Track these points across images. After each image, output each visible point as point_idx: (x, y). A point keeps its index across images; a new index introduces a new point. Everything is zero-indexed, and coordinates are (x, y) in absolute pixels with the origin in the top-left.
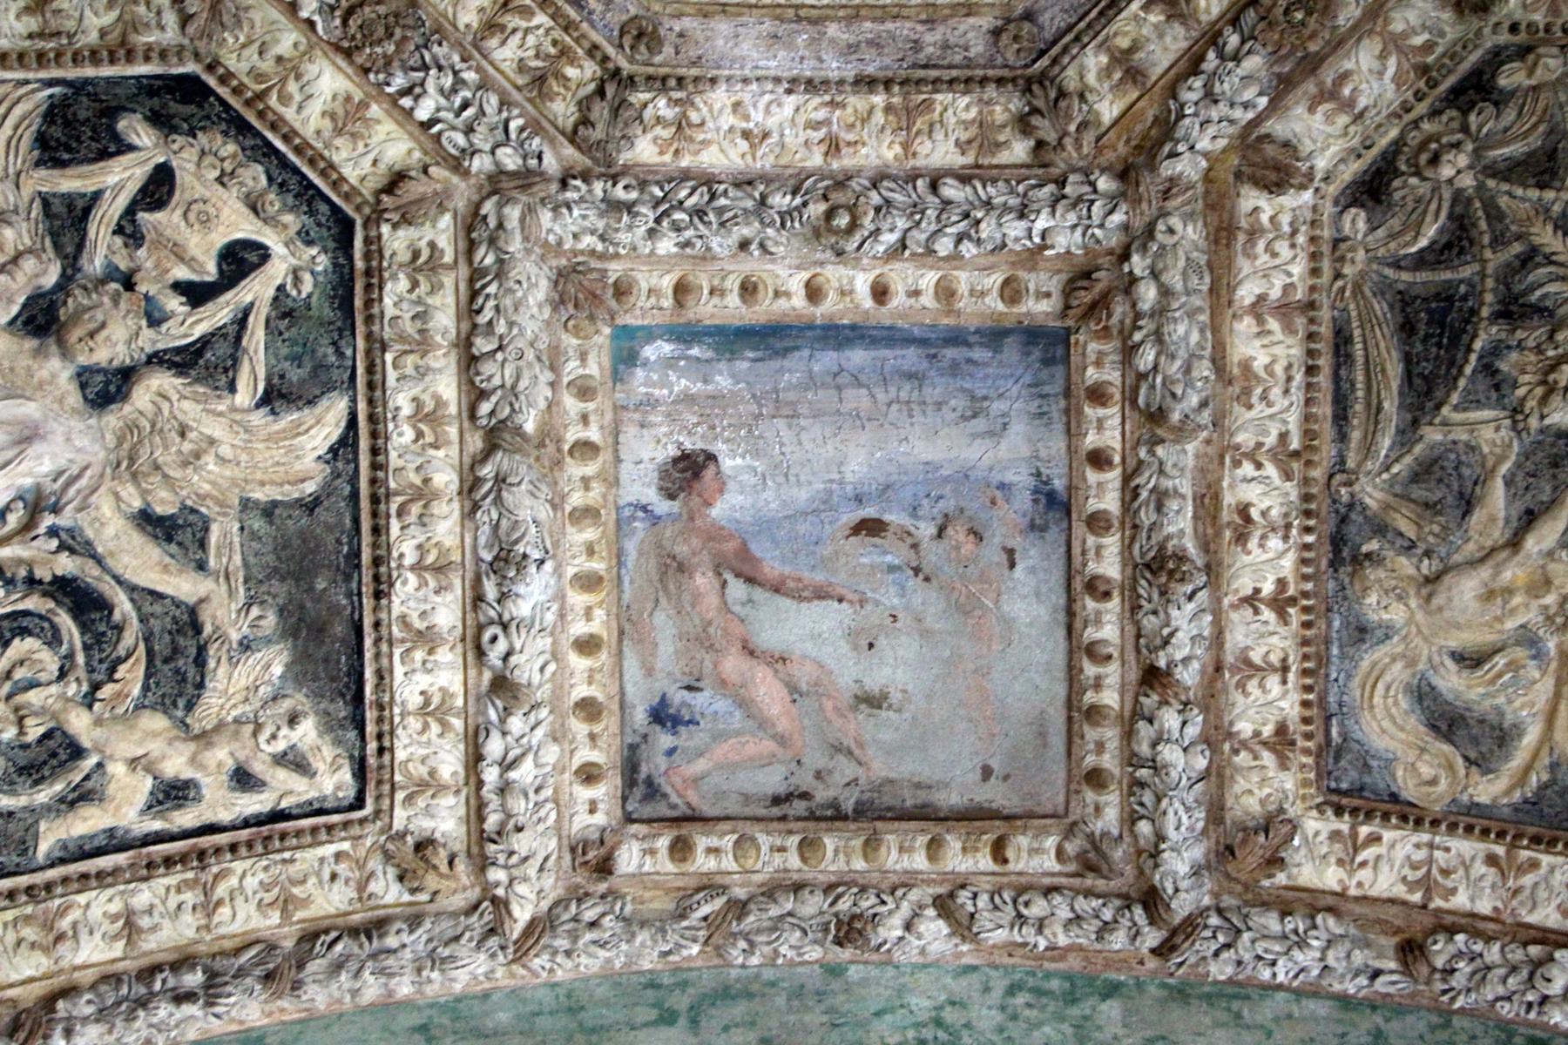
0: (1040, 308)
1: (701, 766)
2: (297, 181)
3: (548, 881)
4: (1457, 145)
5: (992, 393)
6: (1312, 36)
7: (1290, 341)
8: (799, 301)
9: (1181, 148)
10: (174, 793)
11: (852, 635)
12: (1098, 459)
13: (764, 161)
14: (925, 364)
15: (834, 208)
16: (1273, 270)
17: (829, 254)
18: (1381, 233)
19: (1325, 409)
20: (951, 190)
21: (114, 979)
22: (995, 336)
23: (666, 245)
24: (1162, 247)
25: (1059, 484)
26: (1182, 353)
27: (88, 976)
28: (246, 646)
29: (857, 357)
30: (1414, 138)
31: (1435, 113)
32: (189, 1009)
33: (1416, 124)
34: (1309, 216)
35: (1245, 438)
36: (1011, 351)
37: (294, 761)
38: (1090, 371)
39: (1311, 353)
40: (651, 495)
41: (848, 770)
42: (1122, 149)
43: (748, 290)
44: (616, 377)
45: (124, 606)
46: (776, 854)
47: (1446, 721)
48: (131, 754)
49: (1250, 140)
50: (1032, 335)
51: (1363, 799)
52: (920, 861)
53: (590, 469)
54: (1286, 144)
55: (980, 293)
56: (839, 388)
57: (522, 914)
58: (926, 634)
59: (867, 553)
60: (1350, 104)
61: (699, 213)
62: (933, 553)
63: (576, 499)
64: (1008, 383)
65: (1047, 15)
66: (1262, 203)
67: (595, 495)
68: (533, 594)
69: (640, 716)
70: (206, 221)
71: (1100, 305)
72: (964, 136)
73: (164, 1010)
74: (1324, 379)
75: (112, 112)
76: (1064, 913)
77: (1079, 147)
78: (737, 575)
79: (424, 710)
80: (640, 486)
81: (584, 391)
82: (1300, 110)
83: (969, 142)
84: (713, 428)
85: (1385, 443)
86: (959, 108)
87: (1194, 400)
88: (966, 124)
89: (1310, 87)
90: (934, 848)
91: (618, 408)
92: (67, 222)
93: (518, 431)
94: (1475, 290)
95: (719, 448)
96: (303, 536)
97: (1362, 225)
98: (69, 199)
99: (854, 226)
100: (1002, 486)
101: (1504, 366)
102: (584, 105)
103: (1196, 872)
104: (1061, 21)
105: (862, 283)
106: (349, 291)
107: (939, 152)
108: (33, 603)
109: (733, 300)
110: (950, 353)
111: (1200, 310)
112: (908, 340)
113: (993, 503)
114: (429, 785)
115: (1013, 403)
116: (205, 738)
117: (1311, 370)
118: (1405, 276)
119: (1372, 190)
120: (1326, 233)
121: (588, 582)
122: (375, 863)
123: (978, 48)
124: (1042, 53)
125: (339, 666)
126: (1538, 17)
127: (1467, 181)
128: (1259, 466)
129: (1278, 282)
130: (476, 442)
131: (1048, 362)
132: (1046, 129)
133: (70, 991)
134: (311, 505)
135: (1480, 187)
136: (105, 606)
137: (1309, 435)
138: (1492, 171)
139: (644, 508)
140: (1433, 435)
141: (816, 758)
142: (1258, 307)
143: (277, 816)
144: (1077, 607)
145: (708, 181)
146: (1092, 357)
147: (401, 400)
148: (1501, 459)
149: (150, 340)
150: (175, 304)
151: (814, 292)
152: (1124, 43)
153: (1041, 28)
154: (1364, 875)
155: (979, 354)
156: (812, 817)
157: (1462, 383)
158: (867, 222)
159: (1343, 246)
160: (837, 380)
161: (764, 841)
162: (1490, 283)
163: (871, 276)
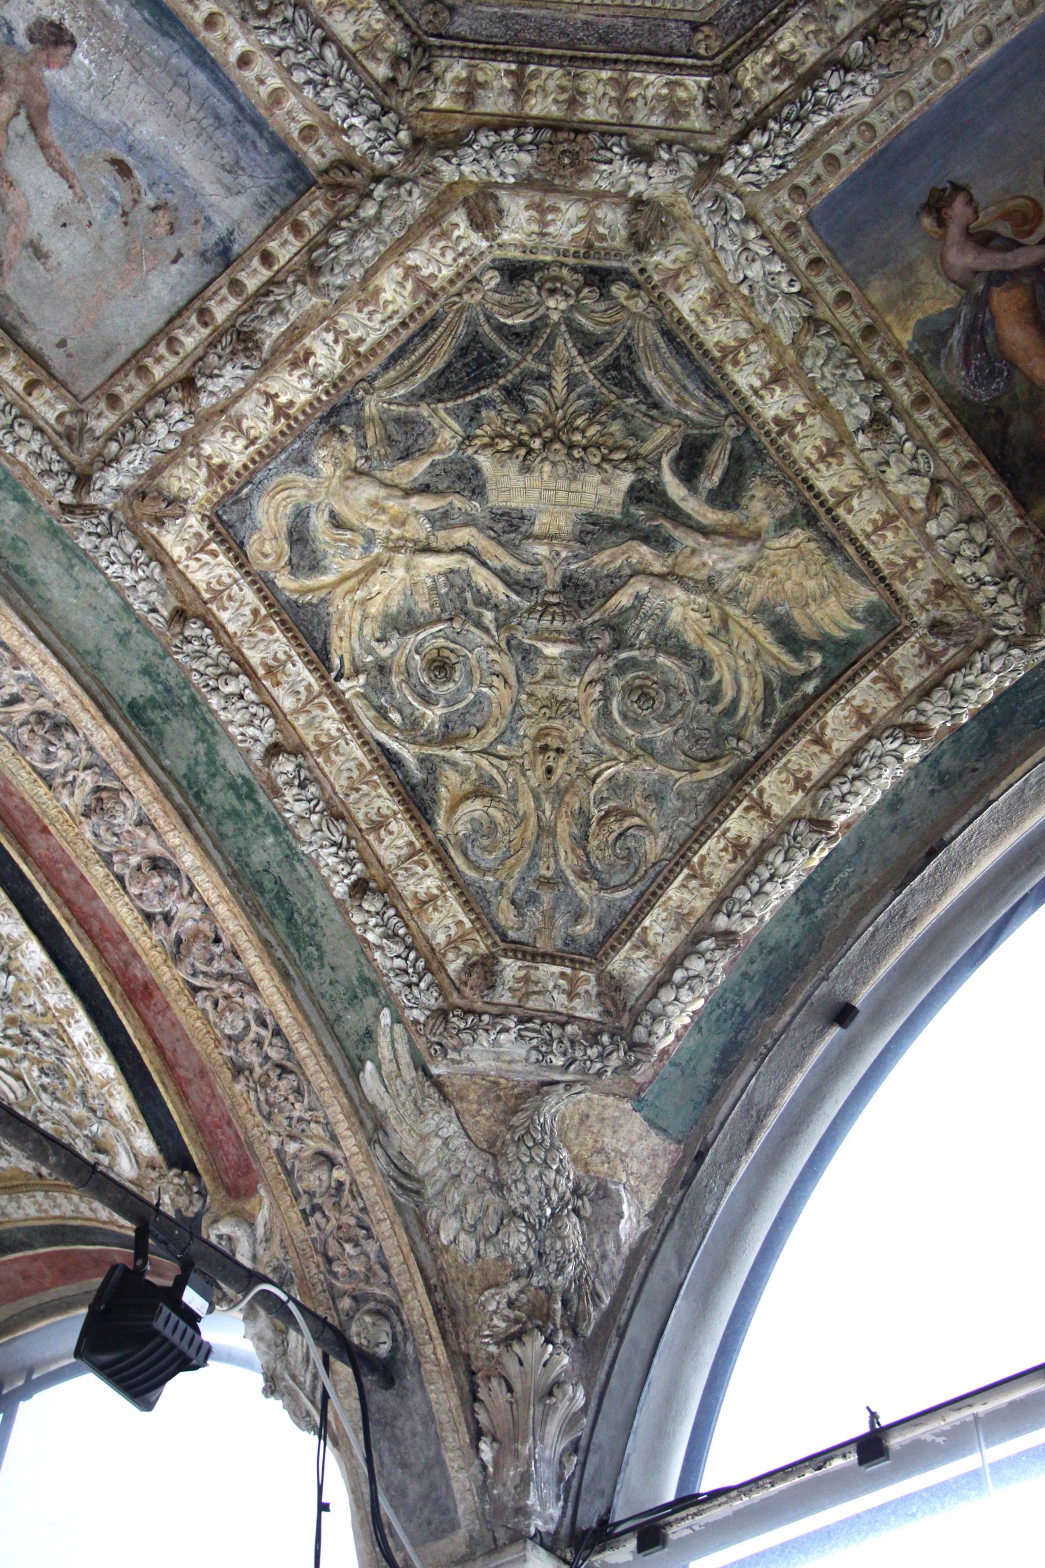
0: (314, 157)
4: (567, 295)
5: (249, 171)
6: (562, 177)
7: (408, 300)
8: (199, 17)
9: (454, 161)
11: (60, 210)
12: (267, 258)
14: (230, 120)
16: (434, 262)
17: (237, 12)
18: (497, 296)
19: (391, 348)
20: (330, 53)
22: (279, 145)
24: (399, 196)
25: (236, 248)
26: (356, 254)
29: (200, 78)
30: (554, 271)
31: (573, 269)
33: (562, 265)
34: (476, 254)
35: (343, 322)
36: (278, 161)
38: (306, 213)
39: (412, 316)
40: (21, 27)
42: (428, 127)
47: (298, 535)
49: (487, 191)
50: (296, 164)
51: (227, 531)
54: (500, 211)
55: (293, 116)
56: (175, 83)
58: (98, 248)
59: (107, 179)
60: (546, 224)
62: (141, 214)
64: (260, 177)
65: (460, 20)
66: (462, 225)
71: (339, 189)
72: (363, 33)
74: (405, 334)
76: (35, 446)
77: (410, 104)
78: (28, 117)
82: (522, 202)
83: (363, 39)
84: (89, 29)
87: (339, 281)
88: (370, 28)
89: (537, 197)
94: (507, 367)
95: (83, 44)
97: (493, 284)
99: (264, 15)
100: (208, 219)
101: (484, 413)
103: (118, 490)
104: (464, 31)
105: (240, 45)
110: (249, 129)
111: (385, 243)
112: (234, 99)
113: (196, 222)
115: (254, 186)
117: (404, 324)
118: (487, 328)
119: (515, 273)
120: (474, 270)
124: (439, 36)
126: (656, 278)
127: (555, 316)
128: (336, 341)
129: (432, 269)
132: (404, 77)
135: (557, 325)
137: (372, 351)
138: (569, 322)
139: (10, 30)
140: (424, 410)
142: (411, 270)
144: (186, 314)
146: (313, 208)
148: (440, 451)
151: (211, 22)
152: (481, 77)
153: (452, 23)
154: (194, 565)
155: (262, 144)
157: (460, 401)
158: (273, 22)
159: (476, 285)
160: (178, 77)
162: (517, 371)
163: (248, 48)
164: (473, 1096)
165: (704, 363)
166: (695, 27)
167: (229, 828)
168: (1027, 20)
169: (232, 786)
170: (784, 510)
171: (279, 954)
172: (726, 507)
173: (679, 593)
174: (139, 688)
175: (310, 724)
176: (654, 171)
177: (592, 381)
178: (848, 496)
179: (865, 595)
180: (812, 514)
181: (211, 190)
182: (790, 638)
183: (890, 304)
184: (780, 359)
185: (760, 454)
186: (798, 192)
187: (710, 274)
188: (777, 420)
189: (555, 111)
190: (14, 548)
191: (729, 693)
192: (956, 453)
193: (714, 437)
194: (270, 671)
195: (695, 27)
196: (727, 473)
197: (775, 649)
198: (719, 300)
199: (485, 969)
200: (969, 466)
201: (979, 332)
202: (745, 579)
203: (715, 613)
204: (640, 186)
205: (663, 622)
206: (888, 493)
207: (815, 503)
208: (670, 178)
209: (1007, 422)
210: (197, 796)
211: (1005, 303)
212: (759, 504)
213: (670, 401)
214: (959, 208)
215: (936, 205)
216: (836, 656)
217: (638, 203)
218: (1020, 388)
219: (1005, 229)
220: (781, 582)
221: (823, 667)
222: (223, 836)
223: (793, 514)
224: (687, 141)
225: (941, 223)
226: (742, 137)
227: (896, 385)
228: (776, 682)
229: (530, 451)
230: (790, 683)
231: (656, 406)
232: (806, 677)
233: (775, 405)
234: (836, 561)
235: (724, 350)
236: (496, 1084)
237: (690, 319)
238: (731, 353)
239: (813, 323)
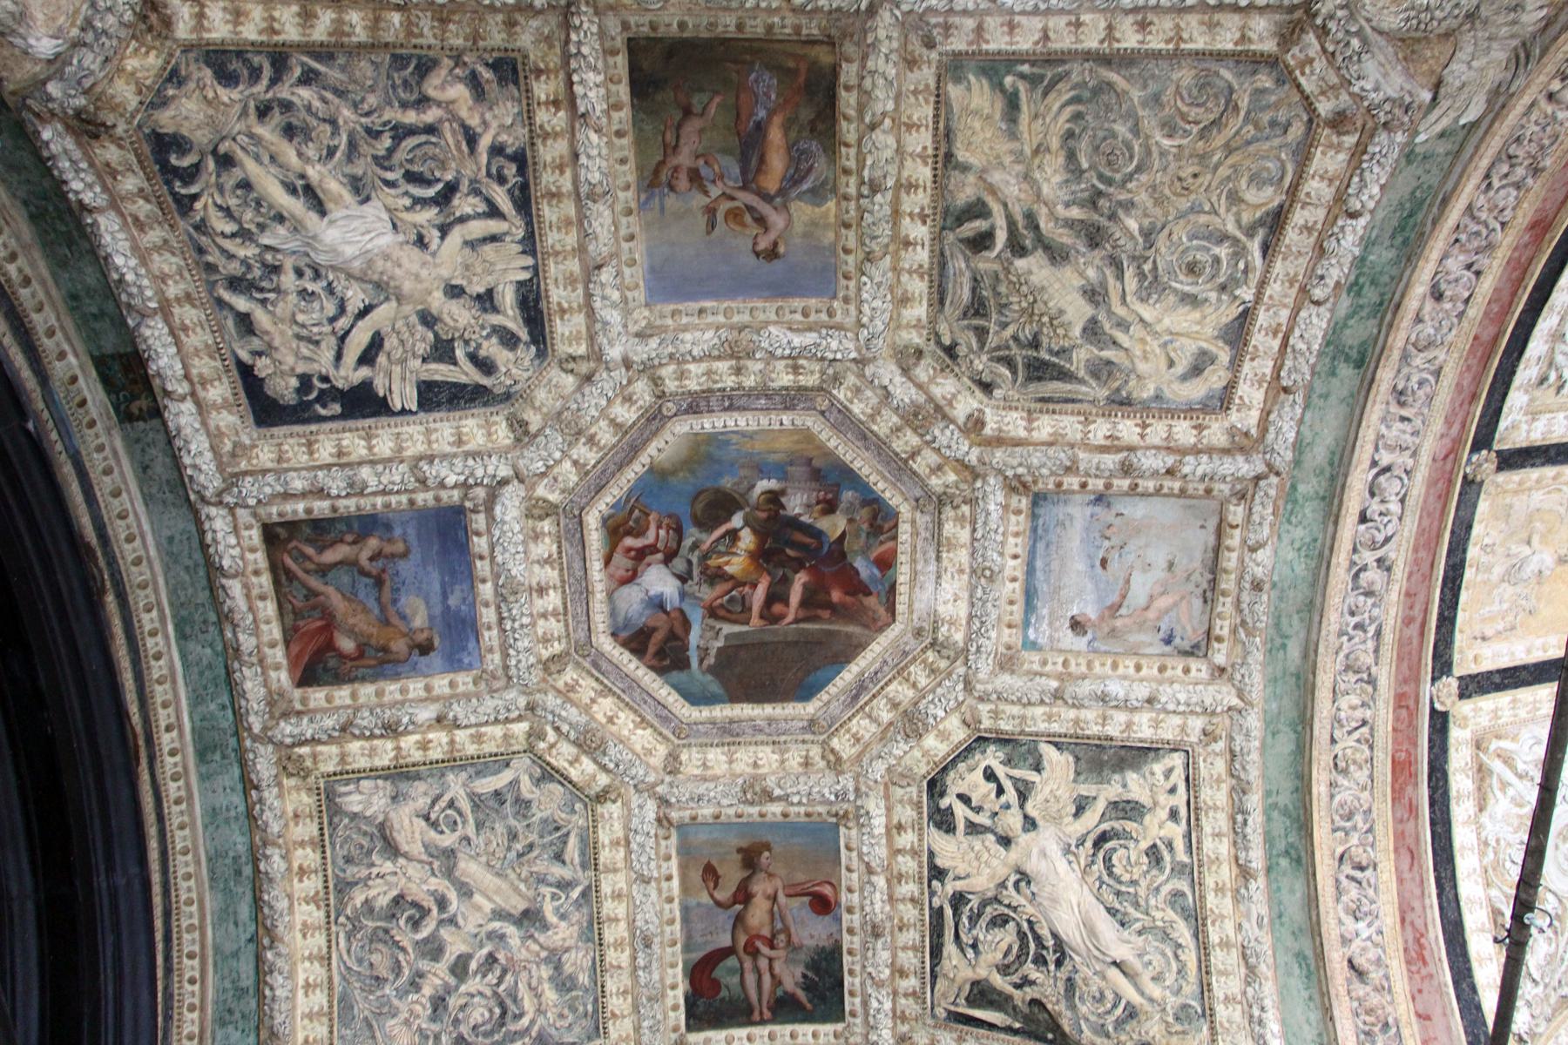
0: (1024, 503)
1: (1189, 628)
2: (965, 753)
3: (1224, 689)
8: (1017, 585)
10: (1174, 815)
11: (1144, 571)
12: (1084, 485)
13: (966, 595)
15: (981, 574)
19: (1070, 406)
20: (979, 535)
21: (1235, 843)
22: (1034, 516)
23: (993, 634)
27: (1233, 851)
28: (1125, 786)
29: (1039, 564)
32: (1250, 822)
35: (1079, 436)
36: (1041, 511)
37: (1168, 773)
40: (1085, 640)
41: (1196, 577)
43: (1011, 603)
44: (1040, 649)
45: (1105, 826)
46: (1225, 606)
47: (1196, 370)
48: (1157, 828)
50: (1035, 504)
51: (1224, 400)
52: (1234, 555)
53: (1073, 662)
55: (1019, 522)
57: (1235, 701)
58: (1147, 546)
59: (1114, 565)
61: (982, 623)
62: (1115, 541)
63: (1083, 669)
67: (1083, 661)
68: (1116, 688)
69: (1168, 649)
70: (976, 786)
71: (1024, 485)
73: (1248, 830)
74: (1058, 407)
75: (939, 810)
79: (1156, 728)
80: (1081, 643)
81: (1045, 663)
85: (1084, 389)
86: (949, 528)
89: (947, 409)
90: (1229, 549)
91: (1052, 649)
92: (973, 829)
93: (1056, 690)
95: (1069, 615)
96: (1088, 762)
98: (967, 827)
102: (942, 657)
103: (1247, 461)
105: (1011, 563)
106: (1003, 741)
107: (964, 535)
108: (1101, 855)
109: (1015, 608)
110: (1040, 531)
112: (1034, 546)
114: (1183, 729)
115: (1059, 511)
116: (1155, 804)
117: (1054, 412)
119: (987, 387)
121: (1115, 666)
122: (1209, 749)
123: (928, 518)
125: (1135, 755)
126: (925, 332)
127: (985, 358)
129: (1019, 422)
130: (1060, 702)
131: (1045, 499)
132: (957, 501)
133: (1237, 859)
134: (1077, 759)
136: (1104, 833)
137: (1079, 413)
140: (1081, 374)
141: (1191, 587)
142: (1029, 430)
143: (1187, 779)
145: (971, 617)
147: (1042, 726)
149: (1015, 809)
150: (1003, 799)
151: (1014, 580)
154: (1255, 402)
155: (1041, 522)
156: (1213, 590)
158: (987, 564)
160: (1047, 571)
161: (1220, 609)
164: (1425, 67)
165: (936, 277)
166: (822, 413)
167: (1386, 279)
168: (680, 307)
169: (1359, 294)
170: (956, 175)
171: (1435, 210)
172: (984, 204)
173: (1046, 189)
174: (1346, 371)
175: (1286, 296)
176: (886, 382)
177: (994, 316)
178: (919, 156)
179: (954, 91)
180: (945, 160)
181: (1079, 524)
182: (1012, 104)
183: (827, 226)
184: (897, 252)
185: (946, 212)
186: (831, 313)
187: (899, 315)
188: (924, 223)
189: (909, 432)
190: (1322, 472)
191: (1070, 110)
192: (848, 131)
193: (961, 241)
194: (1275, 334)
195: (822, 413)
196: (970, 219)
197: (1024, 108)
198: (904, 300)
199: (1339, 122)
200: (847, 118)
201: (794, 179)
202: (1007, 160)
203: (1037, 161)
204: (898, 379)
205: (1067, 181)
206: (898, 142)
207: (939, 165)
208: (882, 371)
209: (812, 123)
210: (1381, 304)
211: (771, 183)
212: (965, 191)
213: (968, 274)
214: (763, 244)
215: (772, 254)
216: (997, 72)
217: (905, 371)
218: (793, 135)
219: (748, 218)
220: (990, 140)
221: (1008, 73)
222: (1392, 278)
223: (955, 168)
224: (862, 376)
225: (775, 244)
226: (834, 360)
227: (852, 190)
228: (1040, 91)
229: (1051, 319)
230: (1033, 80)
231: (975, 280)
232: (1022, 76)
233: (919, 232)
234: (954, 125)
235: (922, 277)
236: (1405, 59)
237: (925, 303)
238: (919, 272)
239: (869, 257)
